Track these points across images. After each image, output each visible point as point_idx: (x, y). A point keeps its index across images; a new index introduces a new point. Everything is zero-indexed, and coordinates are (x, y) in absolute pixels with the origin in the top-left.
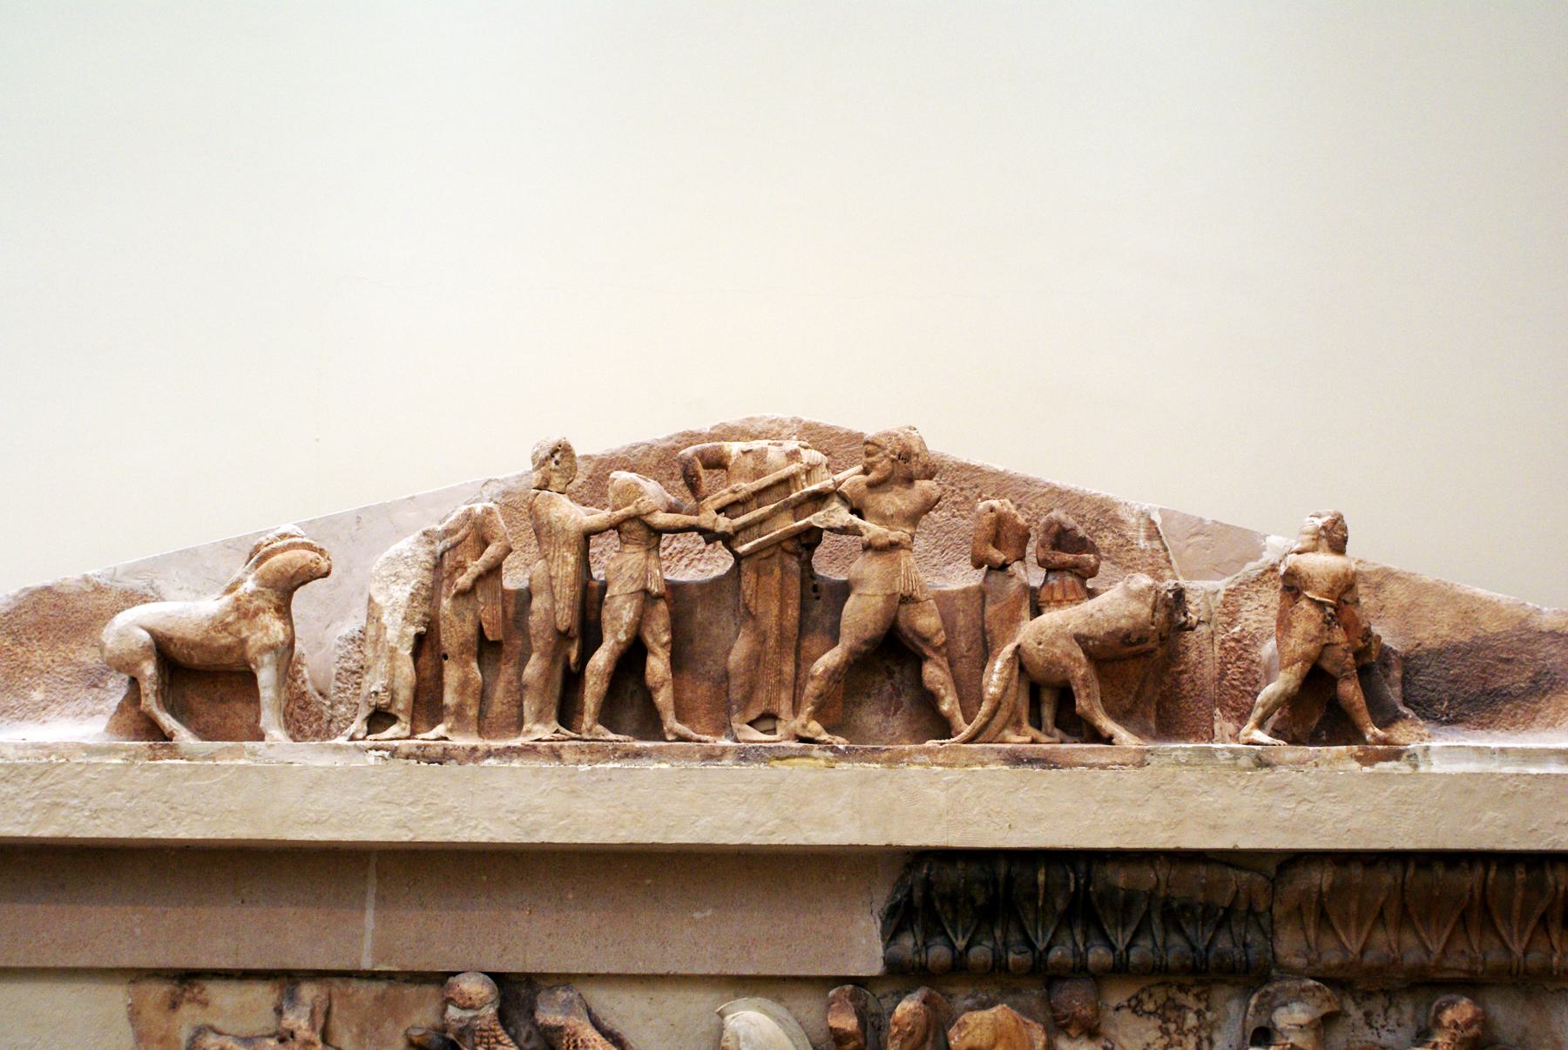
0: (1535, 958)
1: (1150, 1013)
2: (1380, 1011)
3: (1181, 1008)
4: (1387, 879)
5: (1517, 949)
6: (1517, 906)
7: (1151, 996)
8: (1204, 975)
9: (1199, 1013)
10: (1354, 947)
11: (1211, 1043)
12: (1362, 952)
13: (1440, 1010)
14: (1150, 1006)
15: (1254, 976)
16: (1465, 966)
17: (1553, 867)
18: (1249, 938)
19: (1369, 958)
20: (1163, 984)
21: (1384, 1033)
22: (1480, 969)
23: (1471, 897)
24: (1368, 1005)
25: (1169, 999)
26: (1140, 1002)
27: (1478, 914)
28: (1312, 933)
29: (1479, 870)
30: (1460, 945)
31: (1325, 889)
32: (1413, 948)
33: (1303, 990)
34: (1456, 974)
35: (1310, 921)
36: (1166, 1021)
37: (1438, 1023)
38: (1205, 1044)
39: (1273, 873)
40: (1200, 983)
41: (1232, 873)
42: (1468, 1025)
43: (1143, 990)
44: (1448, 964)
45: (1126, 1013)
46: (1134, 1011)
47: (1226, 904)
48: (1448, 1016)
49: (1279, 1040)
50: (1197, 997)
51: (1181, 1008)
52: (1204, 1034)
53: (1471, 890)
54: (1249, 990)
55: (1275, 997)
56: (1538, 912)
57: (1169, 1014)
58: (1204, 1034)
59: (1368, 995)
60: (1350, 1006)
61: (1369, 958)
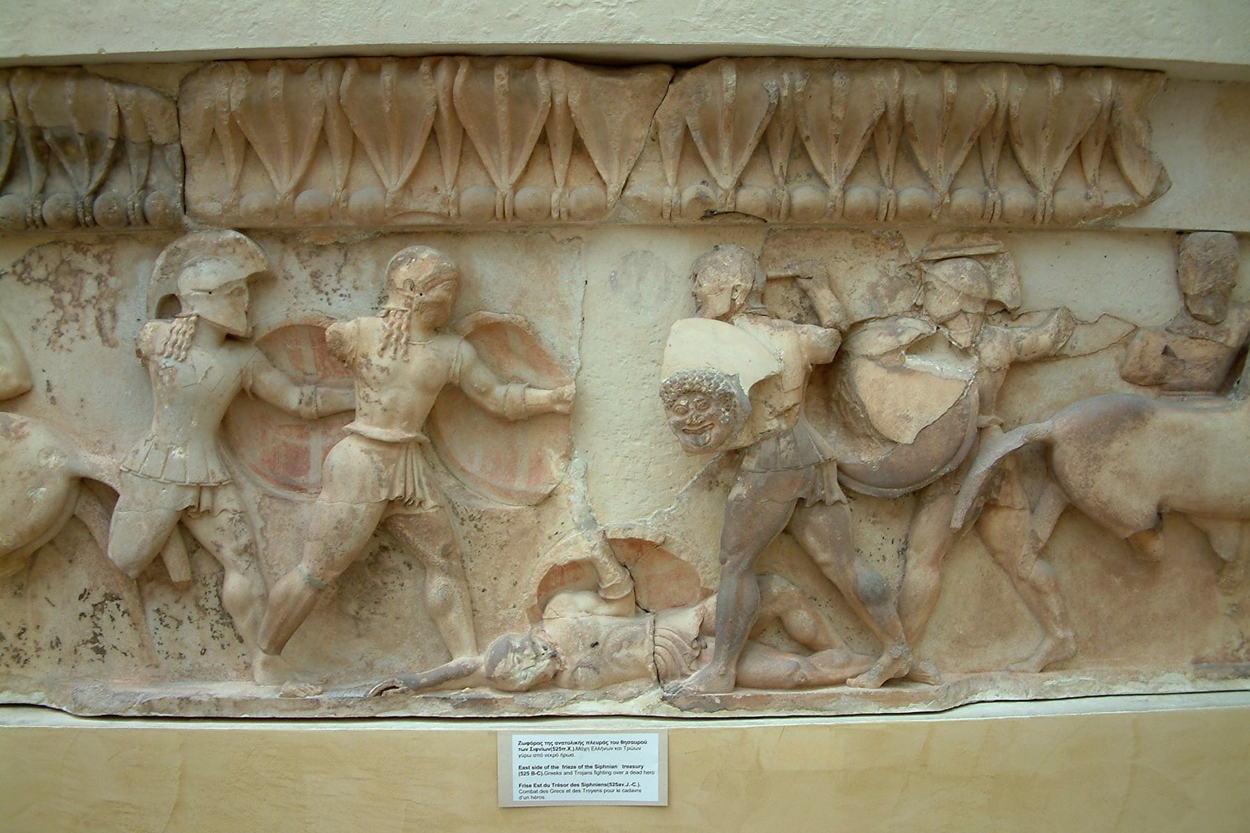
0: (526, 197)
1: (39, 281)
2: (333, 272)
3: (77, 273)
4: (319, 89)
5: (504, 182)
6: (503, 126)
7: (41, 258)
8: (91, 231)
9: (100, 279)
10: (284, 184)
11: (114, 315)
12: (298, 190)
13: (395, 267)
14: (39, 272)
15: (164, 229)
16: (434, 208)
17: (547, 68)
18: (154, 180)
19: (306, 200)
20: (55, 243)
21: (335, 298)
22: (453, 212)
23: (438, 112)
24: (317, 263)
25: (62, 262)
26: (27, 267)
27: (448, 137)
28: (233, 170)
29: (443, 73)
30: (430, 178)
31: (234, 107)
32: (373, 186)
33: (220, 245)
34: (424, 220)
35: (230, 154)
36: (59, 290)
37: (390, 281)
38: (107, 319)
39: (176, 89)
40: (102, 240)
41: (109, 90)
42: (430, 285)
43: (31, 252)
44: (413, 206)
45: (10, 281)
46: (20, 279)
47: (114, 136)
48: (403, 273)
49: (185, 311)
50: (98, 257)
51: (77, 273)
52: (105, 306)
53: (437, 104)
54: (161, 246)
55: (186, 254)
56: (534, 132)
57: (62, 281)
58: (105, 306)
59: (320, 249)
60: (292, 263)
61: (306, 200)
